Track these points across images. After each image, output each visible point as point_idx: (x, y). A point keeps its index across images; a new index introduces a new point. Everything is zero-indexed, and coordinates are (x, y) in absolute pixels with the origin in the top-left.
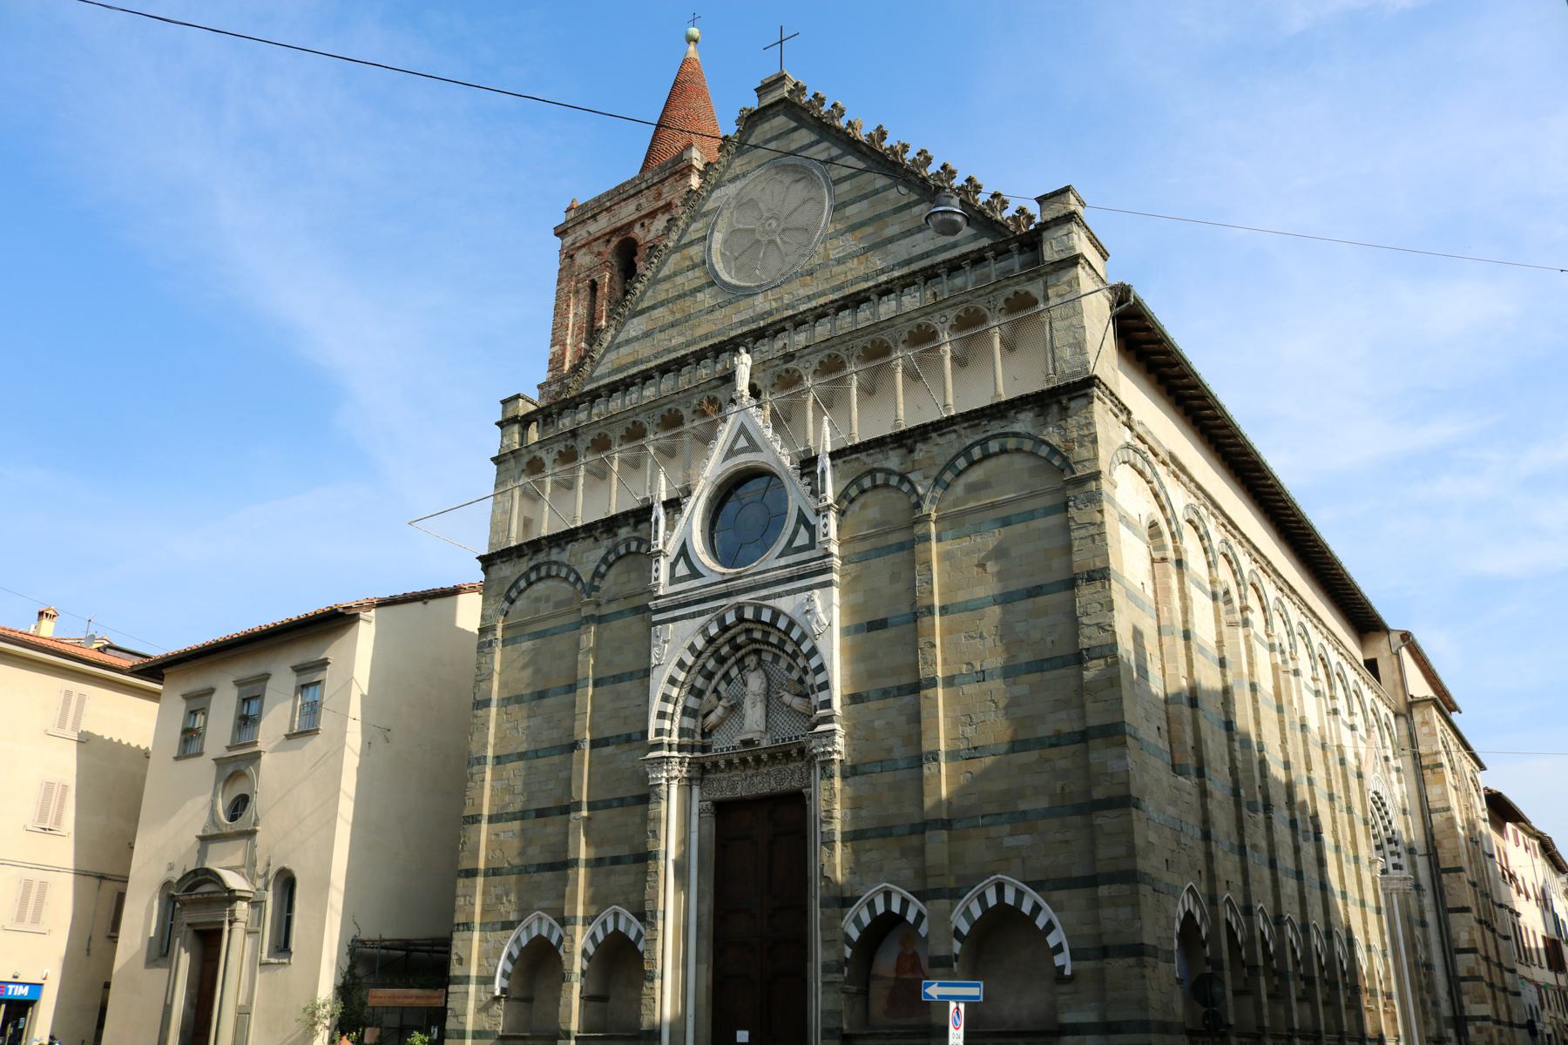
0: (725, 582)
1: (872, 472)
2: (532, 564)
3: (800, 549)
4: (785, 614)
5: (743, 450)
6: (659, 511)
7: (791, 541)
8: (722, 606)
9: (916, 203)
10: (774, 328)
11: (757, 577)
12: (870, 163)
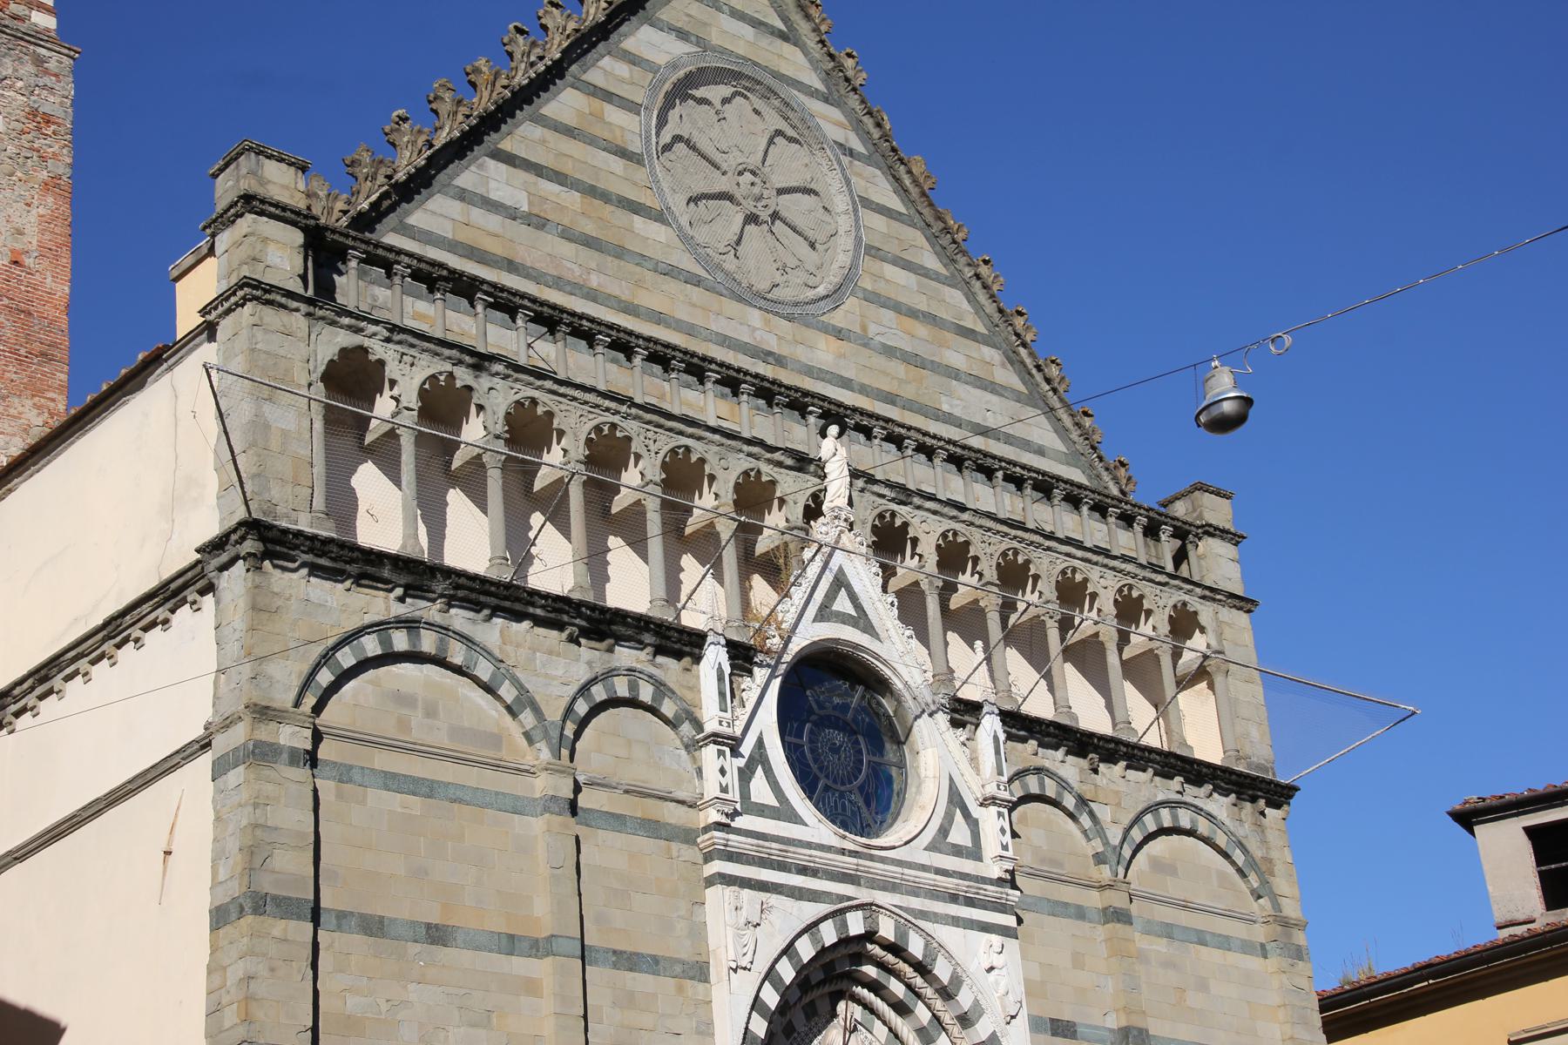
0: (843, 852)
1: (1039, 770)
2: (399, 610)
3: (958, 851)
4: (950, 957)
5: (843, 619)
6: (715, 656)
7: (944, 831)
8: (850, 899)
9: (986, 341)
10: (858, 417)
11: (906, 871)
12: (912, 211)
